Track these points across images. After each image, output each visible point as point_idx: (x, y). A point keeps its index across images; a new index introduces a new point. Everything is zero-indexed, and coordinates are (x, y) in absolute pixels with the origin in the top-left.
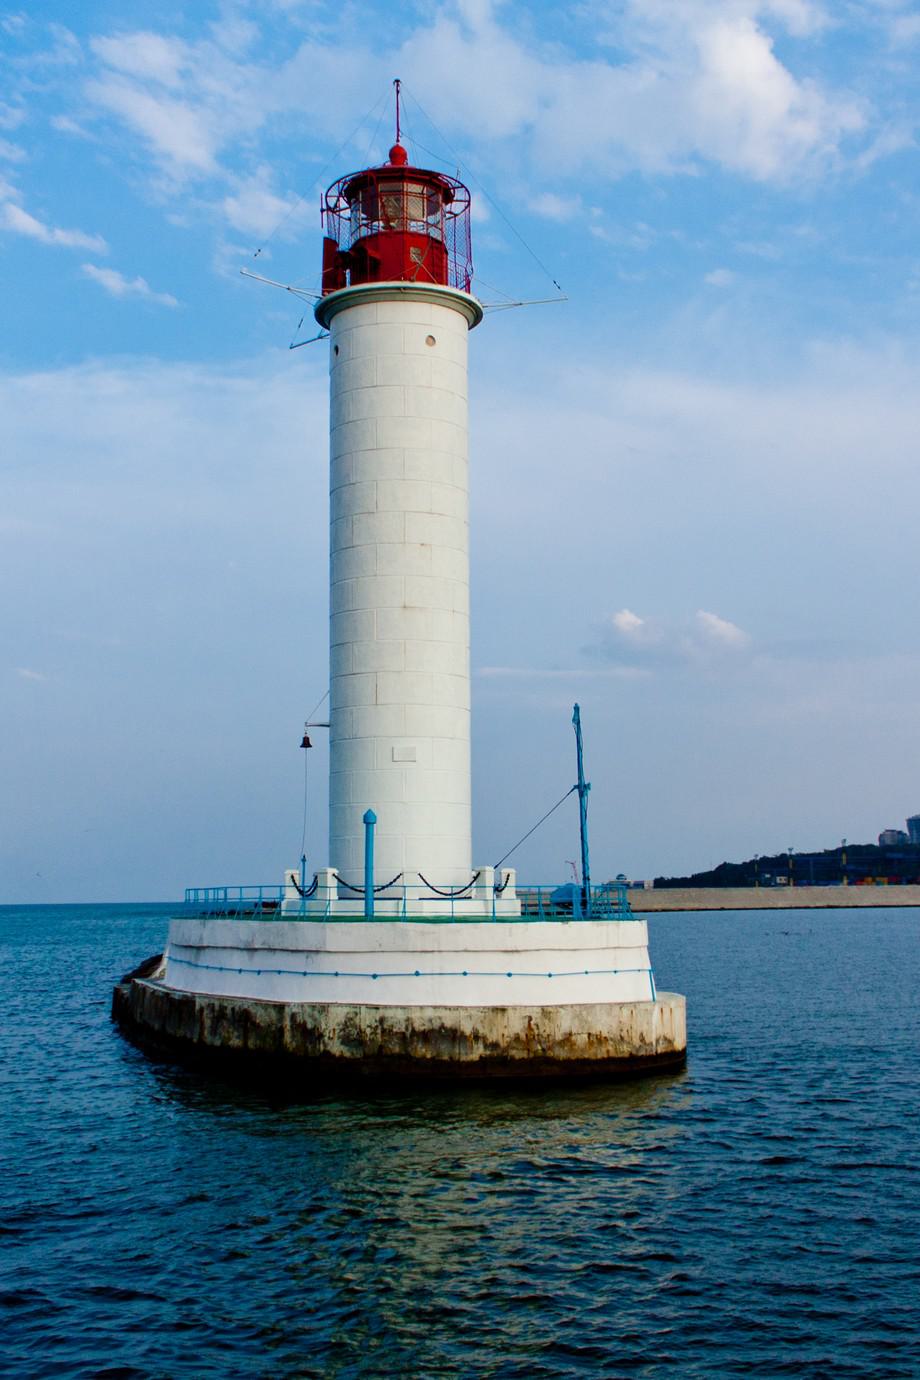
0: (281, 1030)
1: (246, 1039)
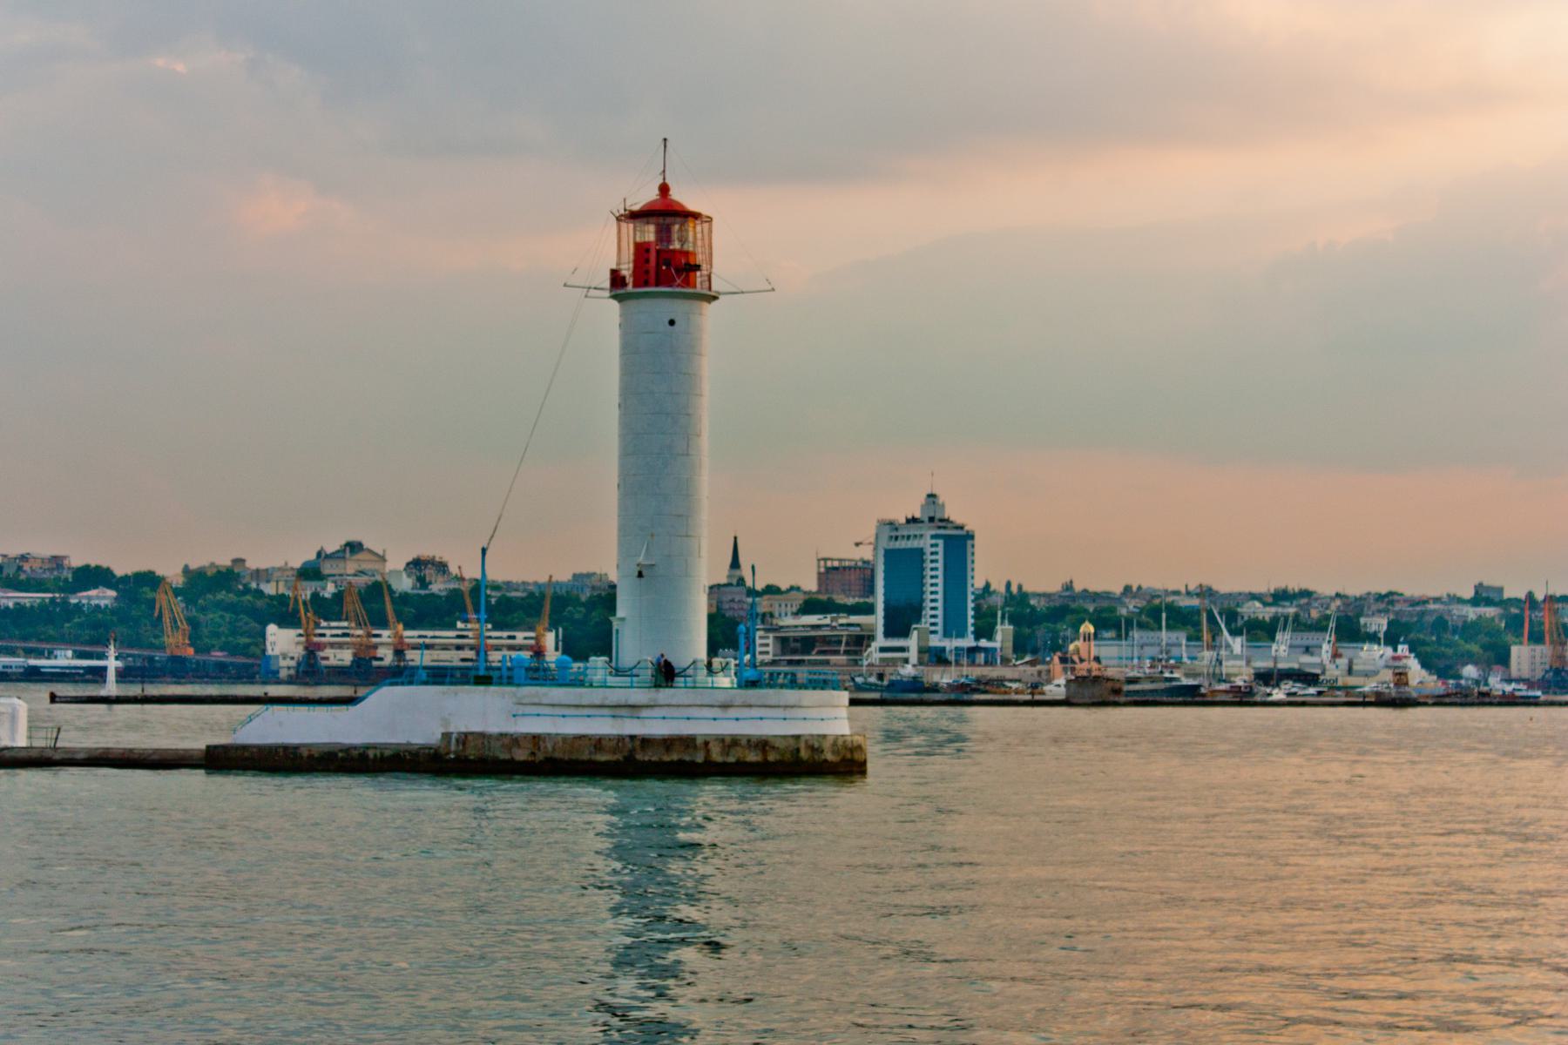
0: (798, 750)
1: (764, 752)
